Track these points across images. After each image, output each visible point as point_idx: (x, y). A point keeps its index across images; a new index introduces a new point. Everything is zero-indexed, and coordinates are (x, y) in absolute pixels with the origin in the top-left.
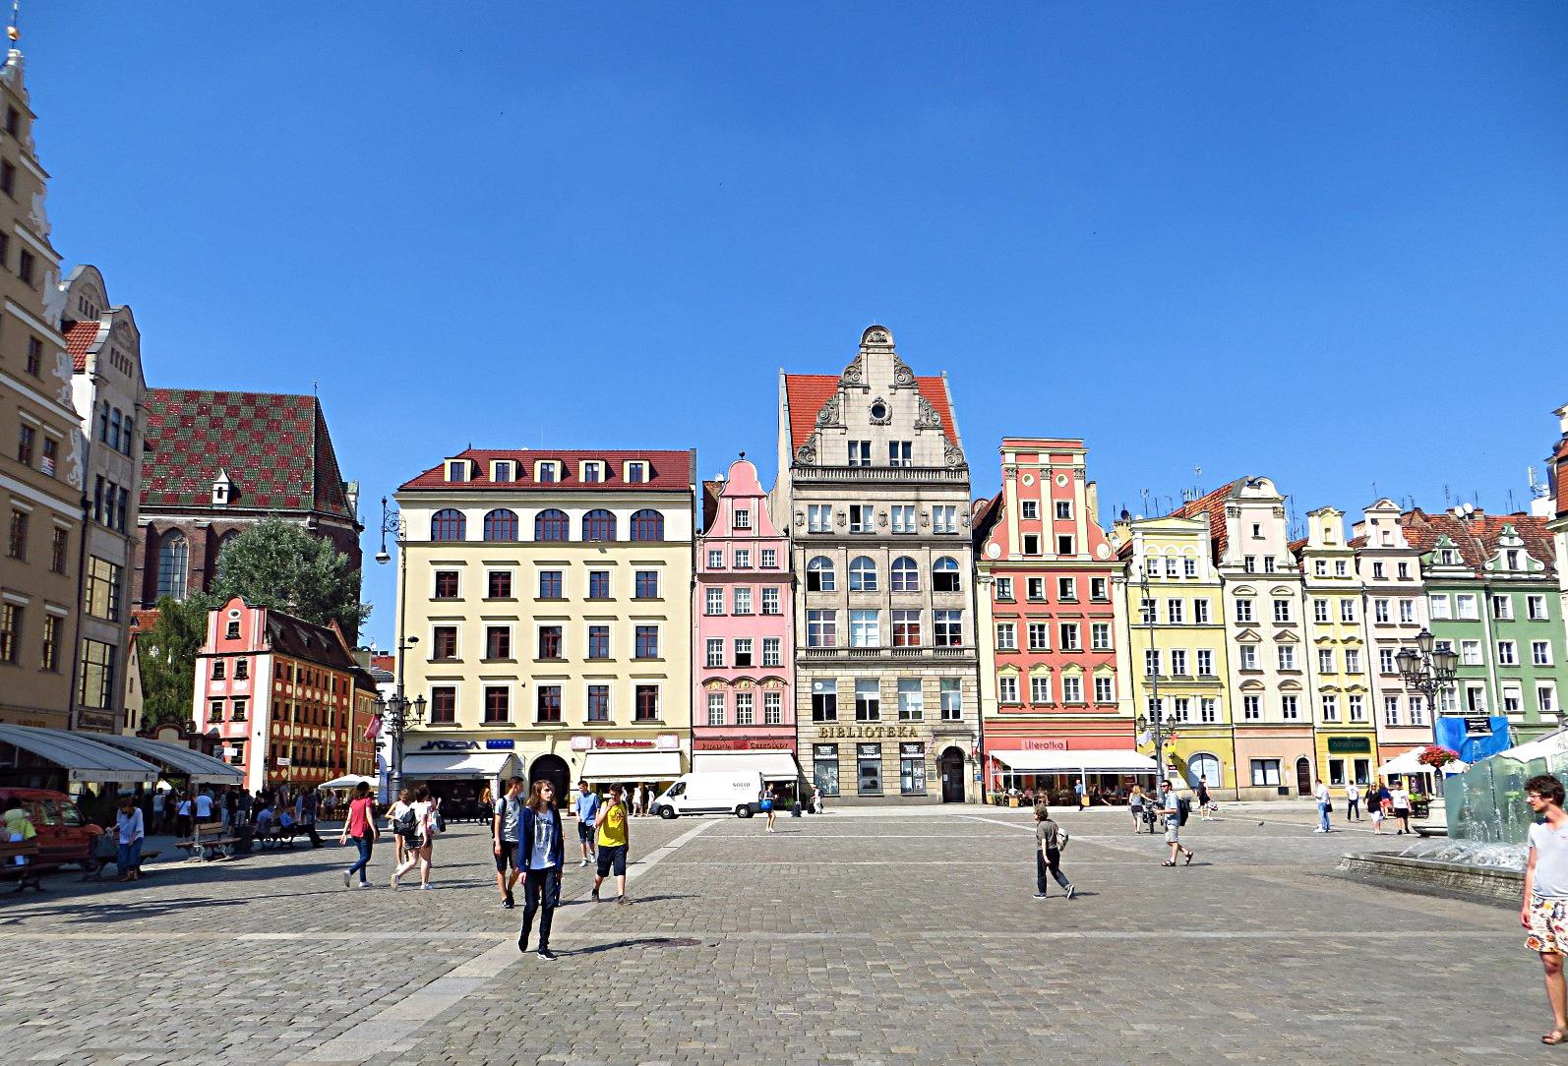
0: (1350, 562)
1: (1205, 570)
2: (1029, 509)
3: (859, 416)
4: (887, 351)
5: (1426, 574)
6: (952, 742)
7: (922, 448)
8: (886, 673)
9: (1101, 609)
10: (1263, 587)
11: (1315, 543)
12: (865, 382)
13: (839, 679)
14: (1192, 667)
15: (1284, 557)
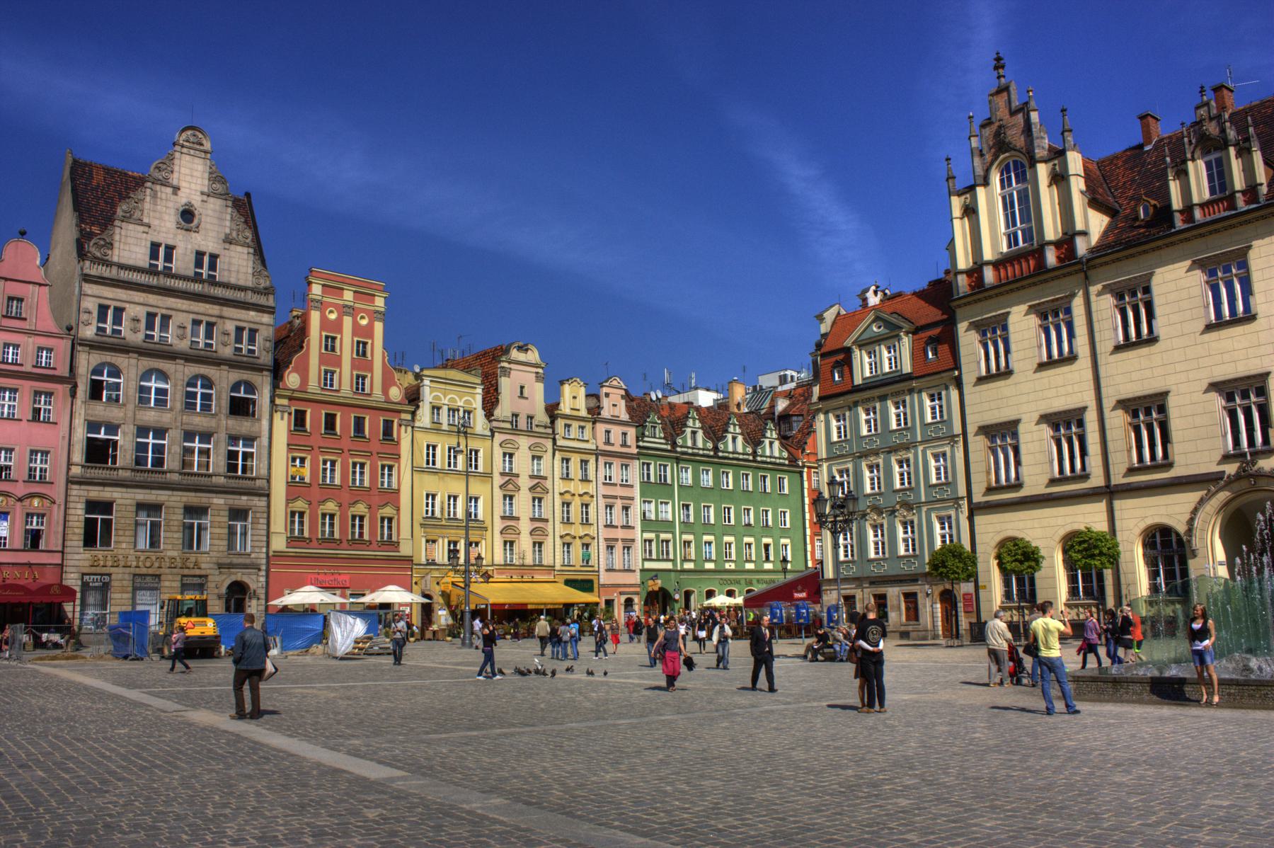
1: (479, 423)
2: (330, 343)
3: (167, 217)
4: (203, 155)
5: (641, 444)
6: (239, 576)
7: (230, 264)
8: (173, 499)
9: (388, 448)
10: (524, 442)
11: (565, 408)
12: (175, 182)
13: (119, 501)
15: (541, 417)
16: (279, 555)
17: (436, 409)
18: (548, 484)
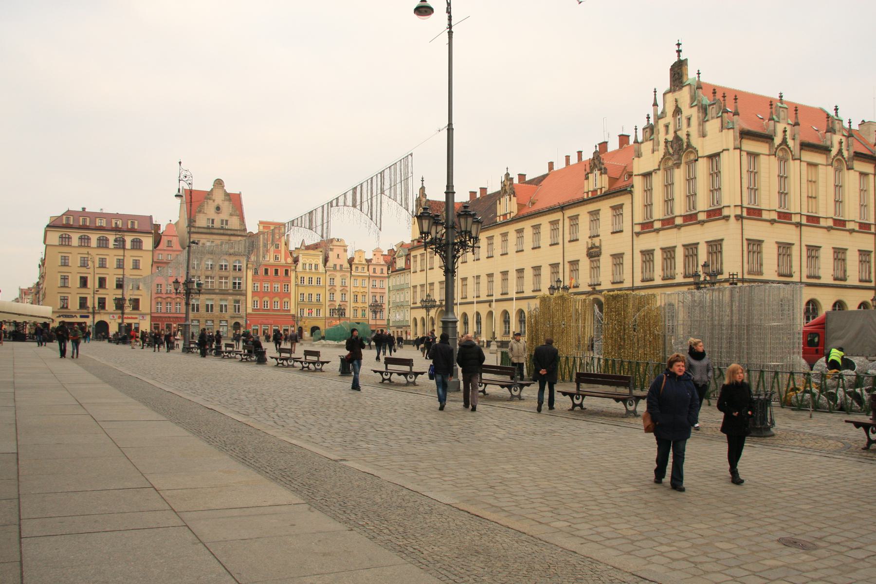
0: (366, 268)
1: (321, 268)
14: (314, 298)
16: (250, 314)
17: (304, 265)
18: (348, 289)
